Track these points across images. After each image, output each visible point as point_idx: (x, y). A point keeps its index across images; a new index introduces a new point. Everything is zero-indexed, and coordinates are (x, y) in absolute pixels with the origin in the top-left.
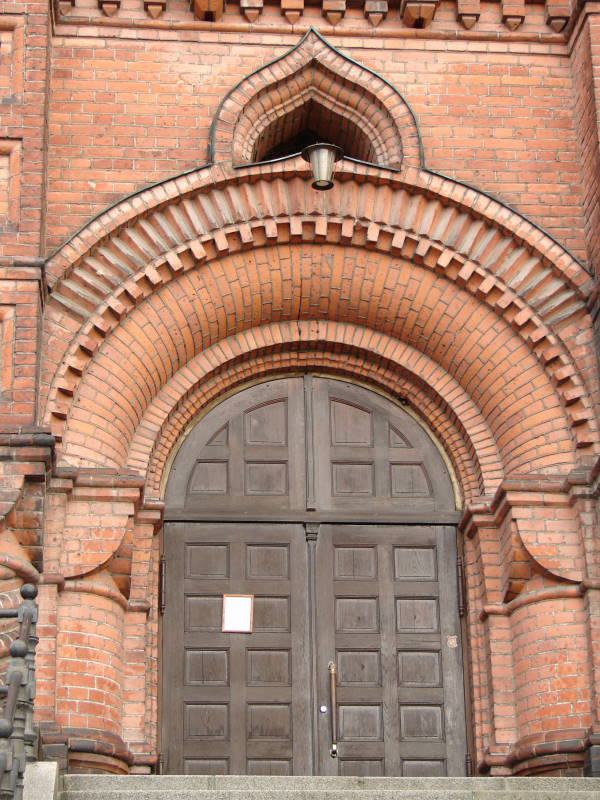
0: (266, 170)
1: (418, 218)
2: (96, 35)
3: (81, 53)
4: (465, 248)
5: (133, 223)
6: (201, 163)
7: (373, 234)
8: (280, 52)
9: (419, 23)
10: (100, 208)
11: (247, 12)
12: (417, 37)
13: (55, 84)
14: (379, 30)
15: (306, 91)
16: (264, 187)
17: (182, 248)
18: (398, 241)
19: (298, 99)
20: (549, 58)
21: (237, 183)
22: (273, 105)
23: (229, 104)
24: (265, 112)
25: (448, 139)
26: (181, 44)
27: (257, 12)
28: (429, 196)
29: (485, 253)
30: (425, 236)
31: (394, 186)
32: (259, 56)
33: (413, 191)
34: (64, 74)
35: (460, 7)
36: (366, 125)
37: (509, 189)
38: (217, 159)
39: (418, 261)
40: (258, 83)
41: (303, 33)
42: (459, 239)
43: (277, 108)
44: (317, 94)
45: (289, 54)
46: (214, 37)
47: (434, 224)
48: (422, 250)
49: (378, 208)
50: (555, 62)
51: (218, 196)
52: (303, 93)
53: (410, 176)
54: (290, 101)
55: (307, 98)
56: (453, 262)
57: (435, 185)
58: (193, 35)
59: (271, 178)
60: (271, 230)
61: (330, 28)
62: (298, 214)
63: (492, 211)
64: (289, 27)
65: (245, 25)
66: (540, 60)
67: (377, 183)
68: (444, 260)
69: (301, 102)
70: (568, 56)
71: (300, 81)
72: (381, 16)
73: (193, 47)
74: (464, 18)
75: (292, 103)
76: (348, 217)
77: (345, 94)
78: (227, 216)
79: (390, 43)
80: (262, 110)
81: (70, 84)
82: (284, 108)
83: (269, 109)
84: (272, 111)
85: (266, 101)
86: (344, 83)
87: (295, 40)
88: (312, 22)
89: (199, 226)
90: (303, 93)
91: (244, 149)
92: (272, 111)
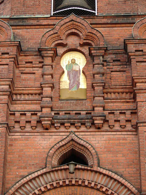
0: (59, 168)
1: (97, 179)
2: (19, 135)
3: (15, 139)
4: (109, 186)
5: (27, 183)
6: (44, 167)
7: (86, 183)
8: (64, 137)
9: (99, 128)
10: (19, 179)
11: (56, 127)
12: (98, 131)
13: (9, 148)
14: (89, 130)
15: (71, 146)
16: (59, 172)
17: (39, 189)
18: (93, 185)
19: (69, 148)
20: (132, 136)
21: (53, 171)
22: (63, 150)
23: (51, 151)
24: (60, 152)
25: (105, 157)
26: (40, 136)
27: (59, 127)
28: (100, 173)
29: (114, 187)
30: (99, 183)
31: (92, 171)
32: (59, 138)
33: (96, 172)
34: (11, 145)
35: (109, 124)
36: (86, 154)
37: (121, 170)
38: (48, 166)
39: (98, 190)
40: (58, 145)
41: (70, 132)
42: (108, 184)
43: (64, 151)
44: (73, 147)
45: (66, 138)
46: (48, 134)
47: (102, 180)
48: (99, 187)
49: (87, 176)
50: (134, 136)
51: (48, 175)
52: (70, 147)
53: (95, 168)
54: (67, 149)
55: (71, 148)
56: (106, 190)
57: (101, 170)
58: (43, 134)
59: (61, 170)
60: (61, 183)
61: (77, 130)
62: (68, 179)
63: (116, 177)
64: (67, 130)
65: (56, 131)
66: (130, 136)
67: (87, 170)
68: (104, 190)
69: (70, 149)
70: (137, 135)
71: (69, 144)
72: (89, 127)
73: (43, 137)
74: (110, 126)
75: (68, 149)
76: (80, 179)
77: (80, 147)
78: (50, 180)
79: (92, 133)
80: (60, 152)
81: (13, 148)
82: (65, 151)
83: (62, 151)
84: (62, 152)
85: (61, 150)
86: (80, 144)
87: (68, 134)
88: (73, 129)
89: (43, 183)
90: (70, 147)
91: (55, 162)
92: (62, 152)
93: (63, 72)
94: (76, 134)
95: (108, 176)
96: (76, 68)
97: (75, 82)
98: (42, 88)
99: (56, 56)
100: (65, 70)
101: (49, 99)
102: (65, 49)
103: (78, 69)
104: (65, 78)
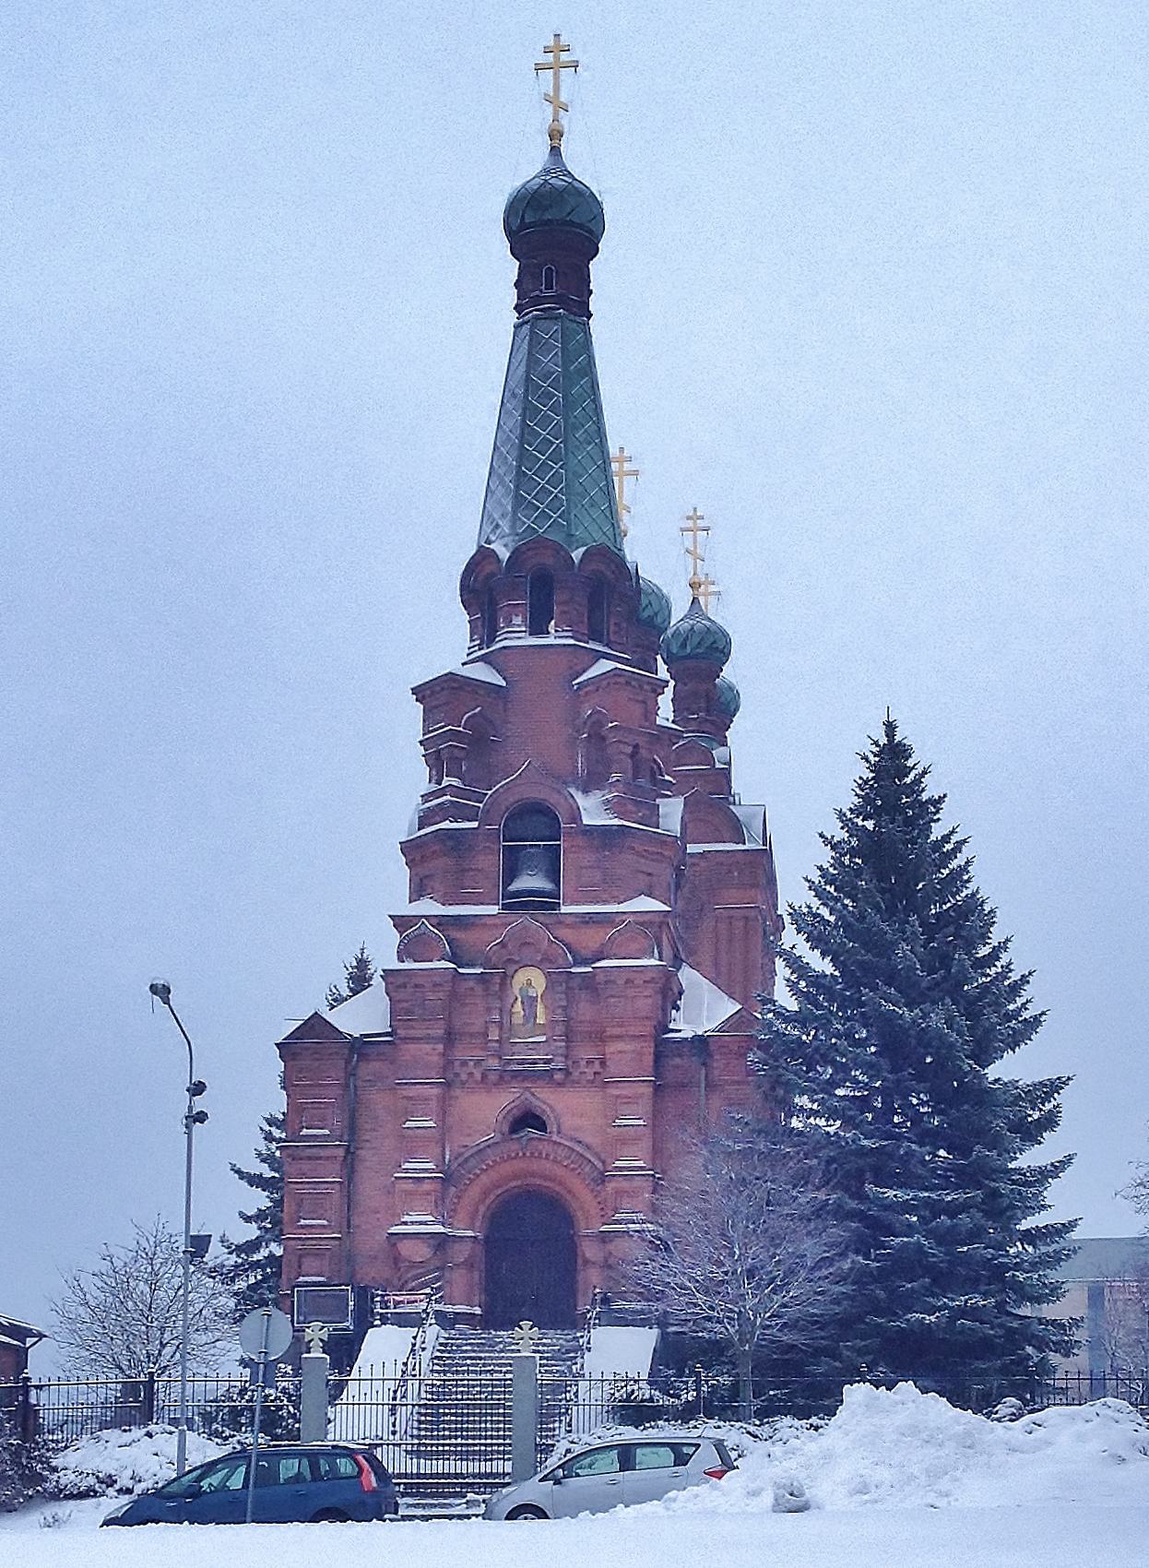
8: (518, 1095)
25: (568, 1122)
33: (555, 1143)
37: (588, 1140)
42: (570, 1156)
53: (555, 1138)
57: (562, 1141)
87: (521, 1091)
91: (506, 1129)
93: (516, 999)
94: (533, 1090)
95: (569, 1148)
96: (532, 993)
97: (530, 1015)
98: (487, 1028)
99: (506, 979)
100: (518, 996)
101: (497, 1045)
102: (516, 967)
103: (535, 995)
104: (518, 1007)
